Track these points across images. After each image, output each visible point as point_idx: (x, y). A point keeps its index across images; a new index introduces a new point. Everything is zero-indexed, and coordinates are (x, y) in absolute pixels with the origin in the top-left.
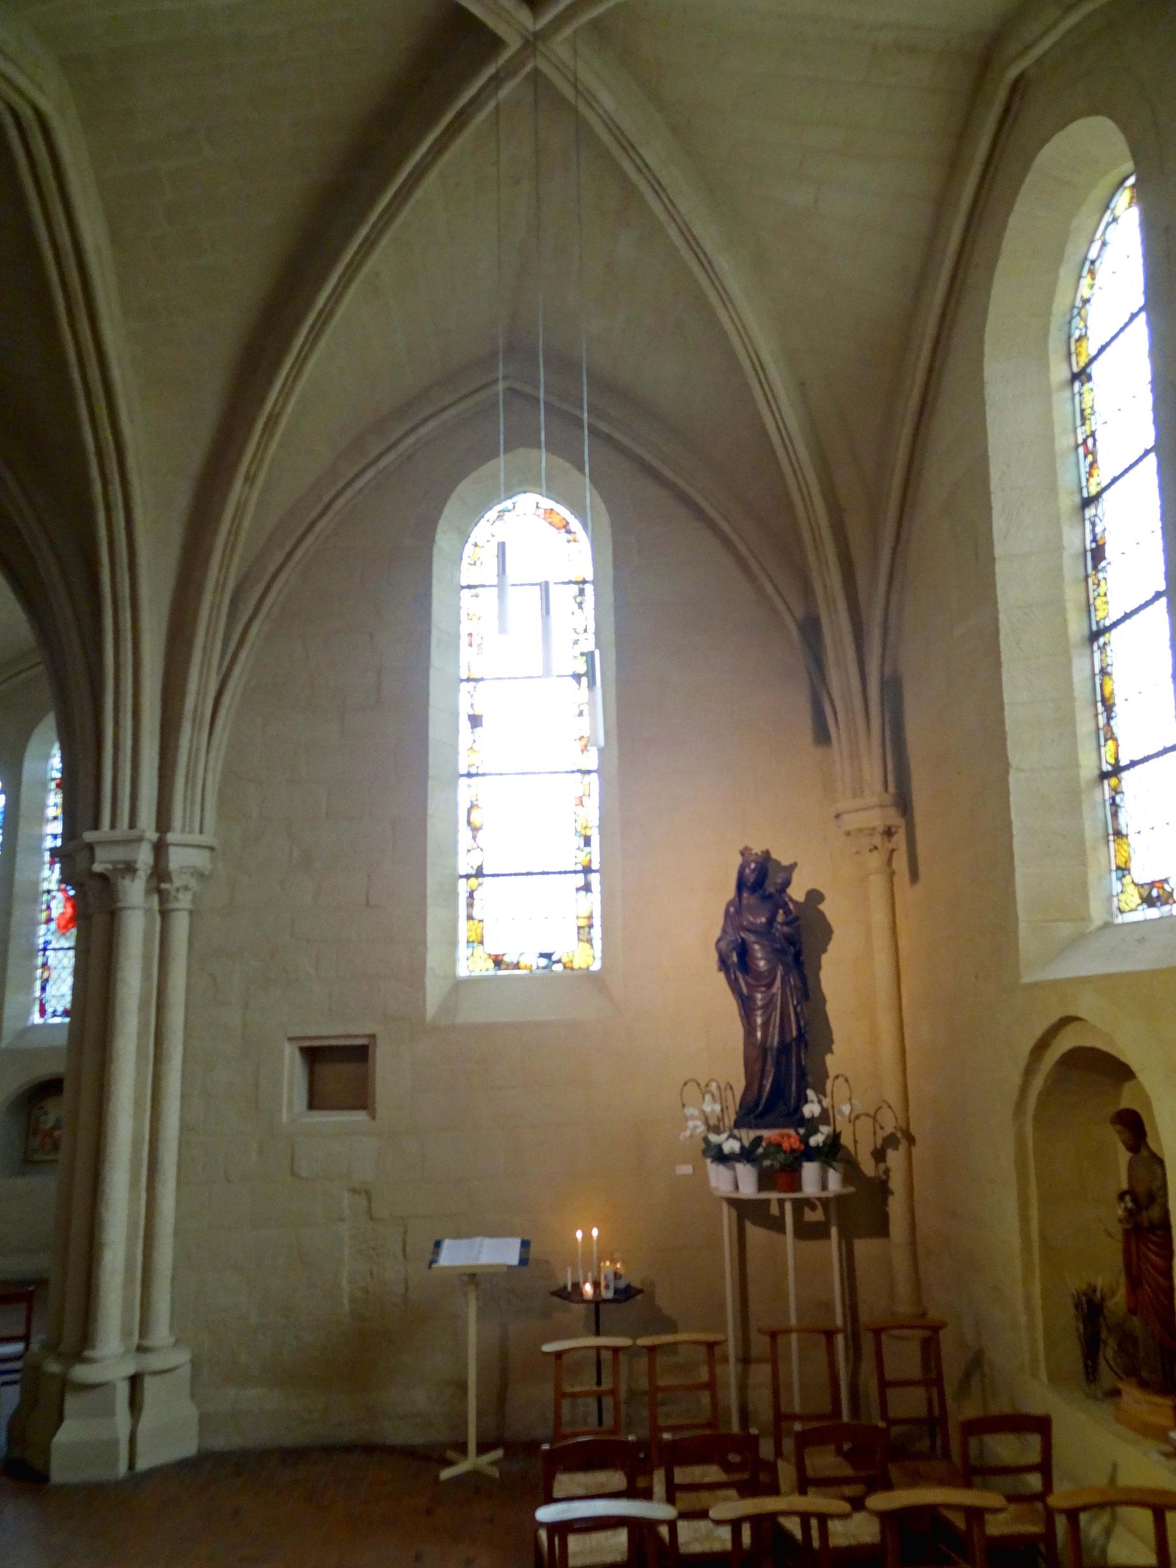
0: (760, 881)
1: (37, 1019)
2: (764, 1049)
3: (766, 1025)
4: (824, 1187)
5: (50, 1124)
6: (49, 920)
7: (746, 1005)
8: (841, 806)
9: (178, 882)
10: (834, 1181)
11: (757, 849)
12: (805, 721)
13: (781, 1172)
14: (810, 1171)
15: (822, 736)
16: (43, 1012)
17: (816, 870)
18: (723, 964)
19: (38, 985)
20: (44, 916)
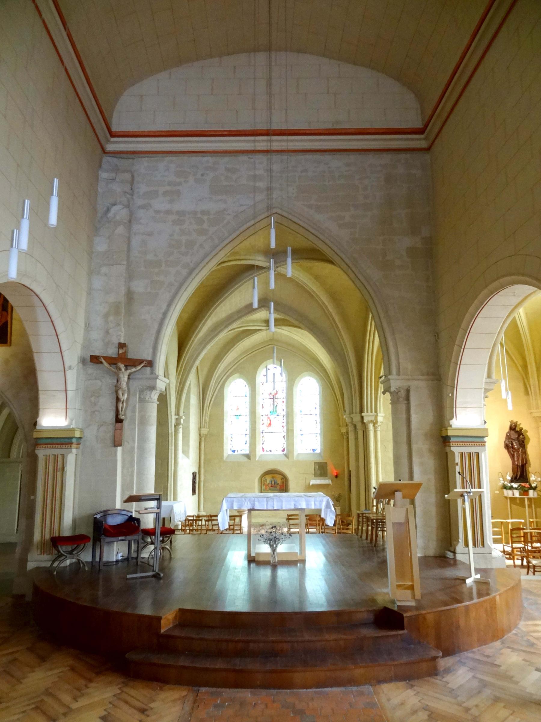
0: (513, 428)
1: (261, 453)
2: (517, 465)
3: (518, 460)
4: (534, 495)
5: (268, 482)
6: (263, 424)
7: (512, 456)
8: (532, 411)
9: (379, 424)
10: (536, 493)
11: (515, 421)
12: (522, 389)
13: (524, 492)
14: (531, 492)
15: (527, 393)
16: (263, 450)
17: (525, 425)
18: (507, 447)
19: (262, 443)
20: (262, 423)
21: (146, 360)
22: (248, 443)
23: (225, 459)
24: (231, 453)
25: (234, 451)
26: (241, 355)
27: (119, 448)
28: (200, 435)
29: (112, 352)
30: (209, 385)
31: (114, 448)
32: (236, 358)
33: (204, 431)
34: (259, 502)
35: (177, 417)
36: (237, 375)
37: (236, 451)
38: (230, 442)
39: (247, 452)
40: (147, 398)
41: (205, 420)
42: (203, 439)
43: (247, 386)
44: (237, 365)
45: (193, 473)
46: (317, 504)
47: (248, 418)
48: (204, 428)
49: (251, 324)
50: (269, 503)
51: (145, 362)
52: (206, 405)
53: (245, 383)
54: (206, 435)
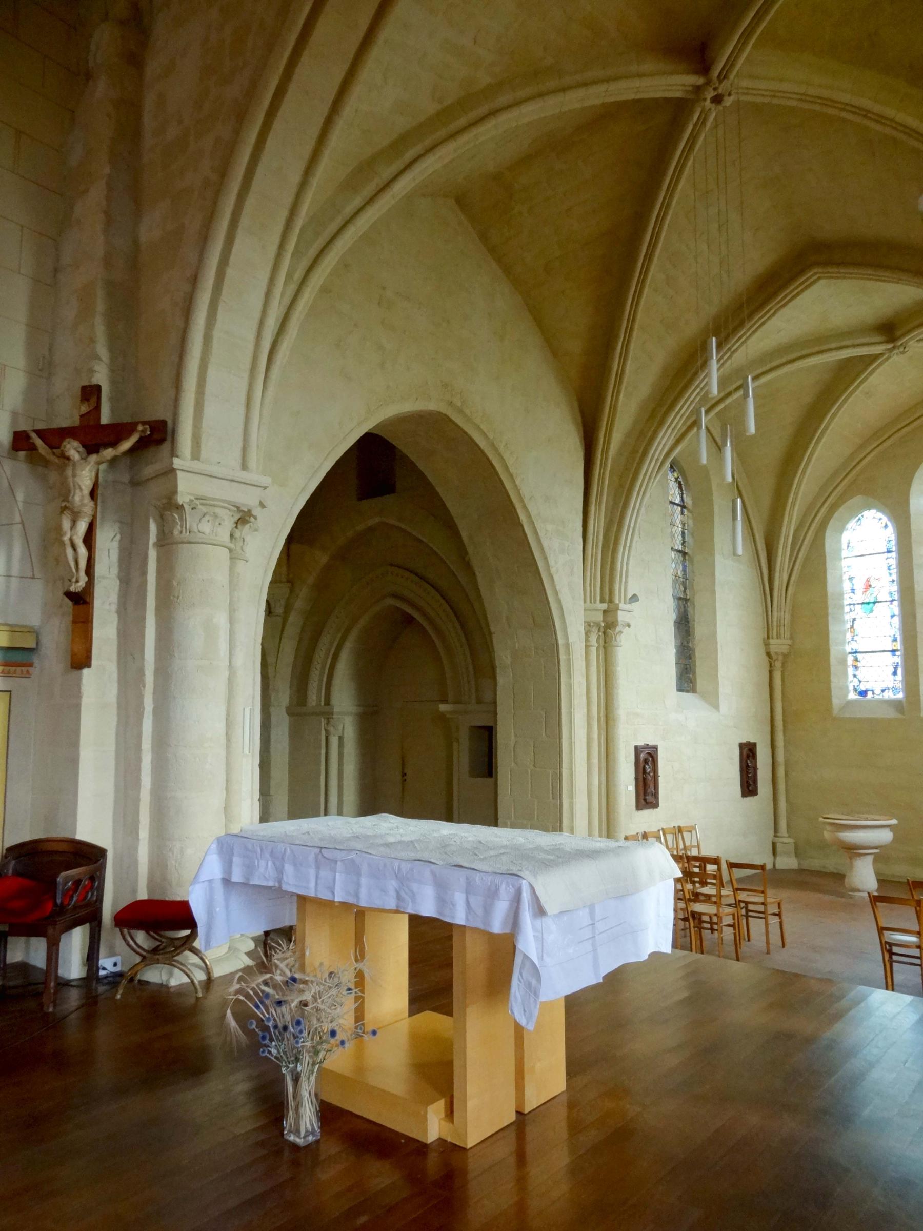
21: (144, 423)
22: (899, 671)
23: (835, 712)
24: (852, 696)
25: (864, 693)
26: (861, 447)
27: (85, 671)
28: (768, 654)
29: (68, 413)
30: (780, 532)
31: (75, 673)
32: (851, 457)
33: (779, 645)
34: (295, 865)
35: (604, 606)
36: (858, 499)
37: (870, 695)
38: (850, 671)
39: (900, 695)
40: (176, 532)
41: (779, 621)
42: (778, 664)
43: (889, 524)
44: (854, 472)
45: (742, 746)
46: (477, 902)
47: (895, 608)
48: (778, 636)
49: (833, 345)
50: (322, 873)
51: (140, 428)
52: (776, 583)
53: (885, 519)
54: (785, 656)
